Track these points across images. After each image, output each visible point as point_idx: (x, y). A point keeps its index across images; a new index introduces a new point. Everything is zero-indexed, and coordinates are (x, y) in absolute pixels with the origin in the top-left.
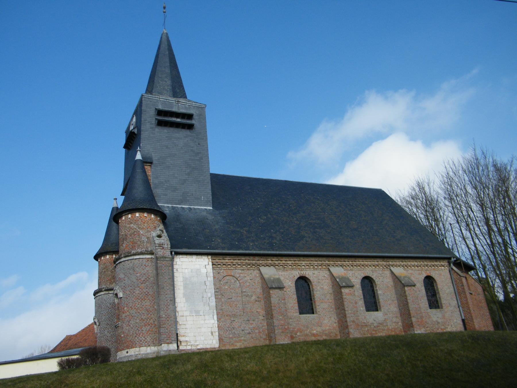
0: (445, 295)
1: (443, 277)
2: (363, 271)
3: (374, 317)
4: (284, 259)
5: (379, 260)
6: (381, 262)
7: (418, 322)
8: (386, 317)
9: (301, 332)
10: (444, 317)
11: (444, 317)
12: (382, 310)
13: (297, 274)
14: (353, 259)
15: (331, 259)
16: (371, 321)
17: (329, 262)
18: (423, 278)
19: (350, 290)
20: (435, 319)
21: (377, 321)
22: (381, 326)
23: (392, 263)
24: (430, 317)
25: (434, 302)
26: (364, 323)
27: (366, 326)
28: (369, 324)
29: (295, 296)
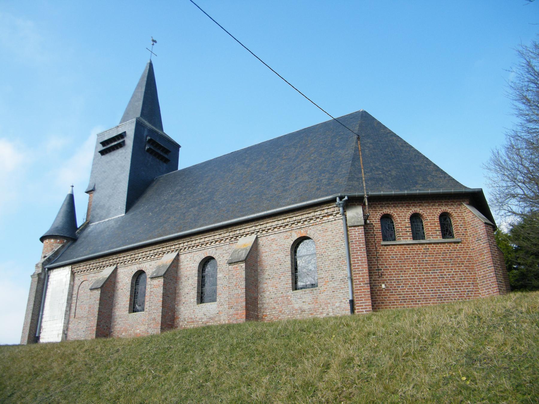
0: (328, 262)
1: (329, 233)
2: (203, 251)
3: (209, 309)
4: (122, 255)
5: (220, 232)
6: (225, 234)
7: (237, 314)
8: (221, 309)
9: (126, 332)
10: (316, 300)
11: (316, 300)
12: (218, 300)
13: (439, 211)
14: (188, 239)
15: (164, 245)
16: (200, 315)
17: (220, 236)
18: (292, 243)
19: (159, 281)
20: (296, 306)
21: (208, 314)
22: (211, 321)
23: (242, 231)
24: (289, 302)
25: (135, 306)
26: (191, 318)
27: (193, 322)
28: (197, 319)
29: (129, 294)
